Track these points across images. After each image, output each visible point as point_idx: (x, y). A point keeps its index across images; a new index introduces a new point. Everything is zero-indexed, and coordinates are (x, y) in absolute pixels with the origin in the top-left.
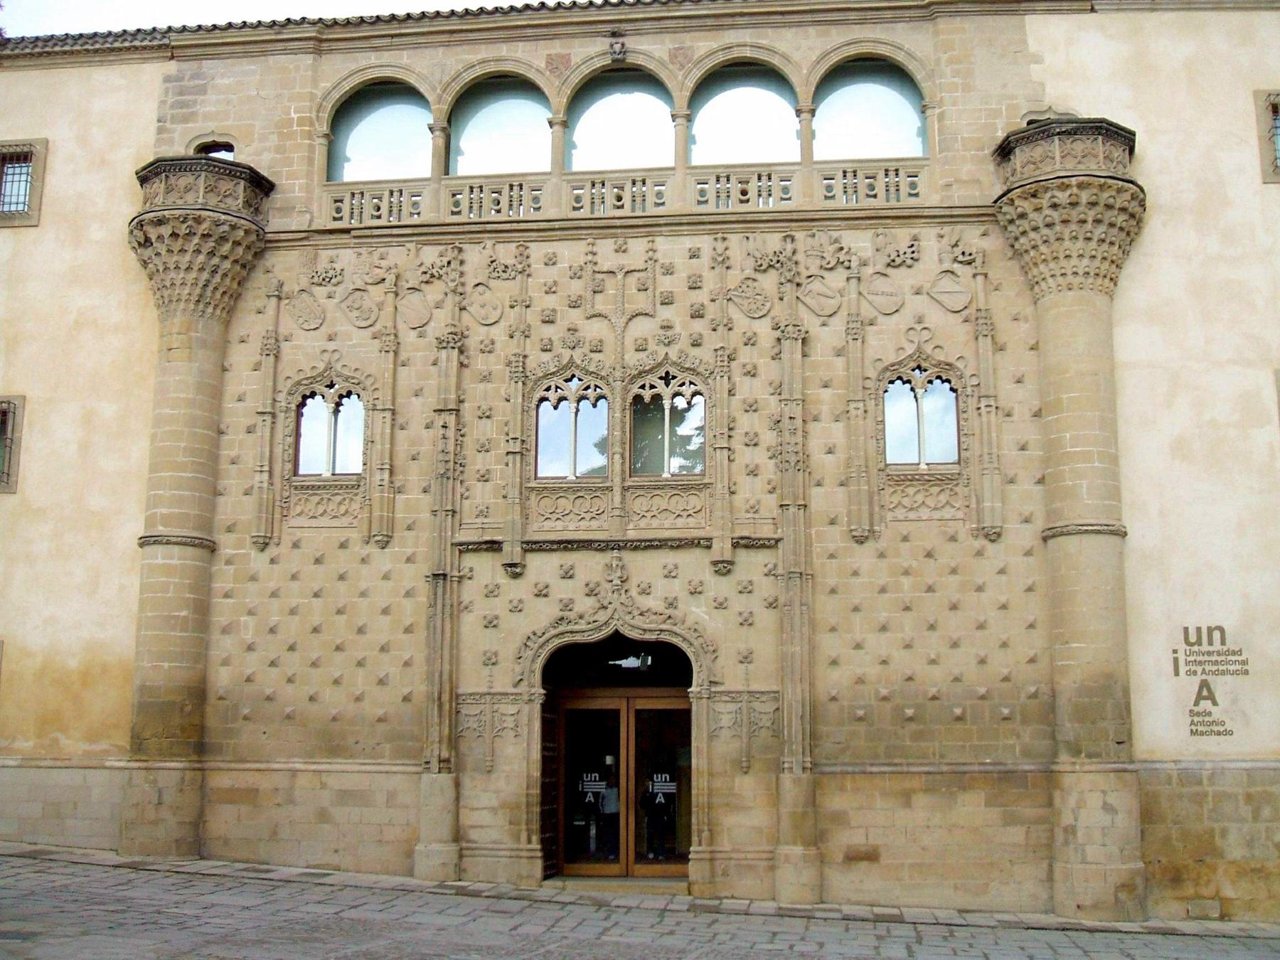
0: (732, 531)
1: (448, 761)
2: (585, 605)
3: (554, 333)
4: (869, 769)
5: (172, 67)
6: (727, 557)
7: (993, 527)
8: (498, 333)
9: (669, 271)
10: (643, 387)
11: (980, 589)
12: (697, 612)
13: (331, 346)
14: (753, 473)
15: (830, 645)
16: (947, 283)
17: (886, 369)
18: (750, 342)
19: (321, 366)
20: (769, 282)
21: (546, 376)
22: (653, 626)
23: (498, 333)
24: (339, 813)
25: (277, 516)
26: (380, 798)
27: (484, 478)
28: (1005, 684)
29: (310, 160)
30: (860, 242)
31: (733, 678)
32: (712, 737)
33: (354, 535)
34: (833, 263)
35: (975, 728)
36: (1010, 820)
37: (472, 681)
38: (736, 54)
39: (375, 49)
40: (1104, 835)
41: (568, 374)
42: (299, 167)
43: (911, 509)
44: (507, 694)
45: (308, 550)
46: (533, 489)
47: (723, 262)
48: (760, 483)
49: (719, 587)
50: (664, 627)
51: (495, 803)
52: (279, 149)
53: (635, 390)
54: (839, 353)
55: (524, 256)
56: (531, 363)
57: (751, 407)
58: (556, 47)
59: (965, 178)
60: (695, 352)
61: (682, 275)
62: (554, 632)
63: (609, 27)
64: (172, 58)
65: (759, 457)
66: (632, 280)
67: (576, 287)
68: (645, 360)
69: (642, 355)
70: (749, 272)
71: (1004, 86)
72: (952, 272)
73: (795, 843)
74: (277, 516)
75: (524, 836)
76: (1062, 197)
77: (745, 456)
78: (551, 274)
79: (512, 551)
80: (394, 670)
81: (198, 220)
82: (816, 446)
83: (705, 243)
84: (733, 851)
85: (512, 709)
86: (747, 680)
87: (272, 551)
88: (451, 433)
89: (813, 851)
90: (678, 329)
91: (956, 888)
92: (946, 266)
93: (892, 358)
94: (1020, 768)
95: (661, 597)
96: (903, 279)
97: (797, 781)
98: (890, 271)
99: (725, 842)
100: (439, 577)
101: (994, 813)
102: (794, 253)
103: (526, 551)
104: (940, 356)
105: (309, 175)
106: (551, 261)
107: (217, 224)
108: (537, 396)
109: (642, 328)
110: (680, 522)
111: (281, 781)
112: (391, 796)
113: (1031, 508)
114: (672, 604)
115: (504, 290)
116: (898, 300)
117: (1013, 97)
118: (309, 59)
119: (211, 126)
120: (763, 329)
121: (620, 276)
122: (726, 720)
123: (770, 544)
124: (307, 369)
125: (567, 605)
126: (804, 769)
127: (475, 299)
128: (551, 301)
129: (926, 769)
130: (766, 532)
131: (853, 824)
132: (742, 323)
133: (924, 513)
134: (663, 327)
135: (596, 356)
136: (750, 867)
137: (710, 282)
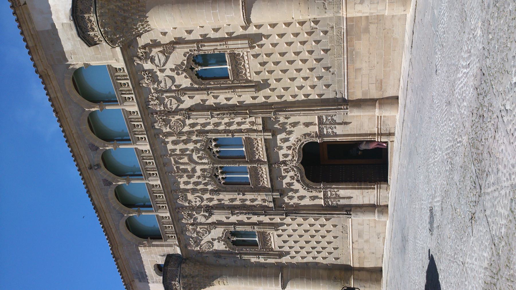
0: (260, 131)
2: (292, 173)
4: (346, 83)
7: (249, 44)
16: (157, 61)
19: (223, 243)
24: (366, 237)
25: (271, 253)
26: (360, 227)
29: (157, 246)
31: (315, 129)
32: (336, 135)
33: (275, 233)
36: (367, 30)
40: (373, 3)
42: (160, 249)
43: (246, 70)
45: (282, 244)
51: (361, 197)
52: (156, 254)
54: (191, 97)
59: (111, 54)
64: (133, 281)
71: (69, 39)
73: (375, 112)
79: (276, 195)
80: (317, 223)
81: (184, 284)
85: (329, 193)
89: (377, 105)
90: (192, 148)
91: (394, 50)
94: (345, 27)
95: (288, 148)
97: (351, 112)
99: (374, 130)
101: (364, 37)
104: (185, 62)
105: (162, 246)
108: (223, 185)
110: (260, 145)
111: (356, 252)
112: (359, 224)
115: (190, 196)
116: (167, 78)
117: (72, 35)
120: (188, 122)
122: (330, 130)
124: (225, 246)
125: (292, 178)
126: (347, 109)
130: (260, 121)
132: (186, 129)
133: (247, 66)
136: (383, 122)
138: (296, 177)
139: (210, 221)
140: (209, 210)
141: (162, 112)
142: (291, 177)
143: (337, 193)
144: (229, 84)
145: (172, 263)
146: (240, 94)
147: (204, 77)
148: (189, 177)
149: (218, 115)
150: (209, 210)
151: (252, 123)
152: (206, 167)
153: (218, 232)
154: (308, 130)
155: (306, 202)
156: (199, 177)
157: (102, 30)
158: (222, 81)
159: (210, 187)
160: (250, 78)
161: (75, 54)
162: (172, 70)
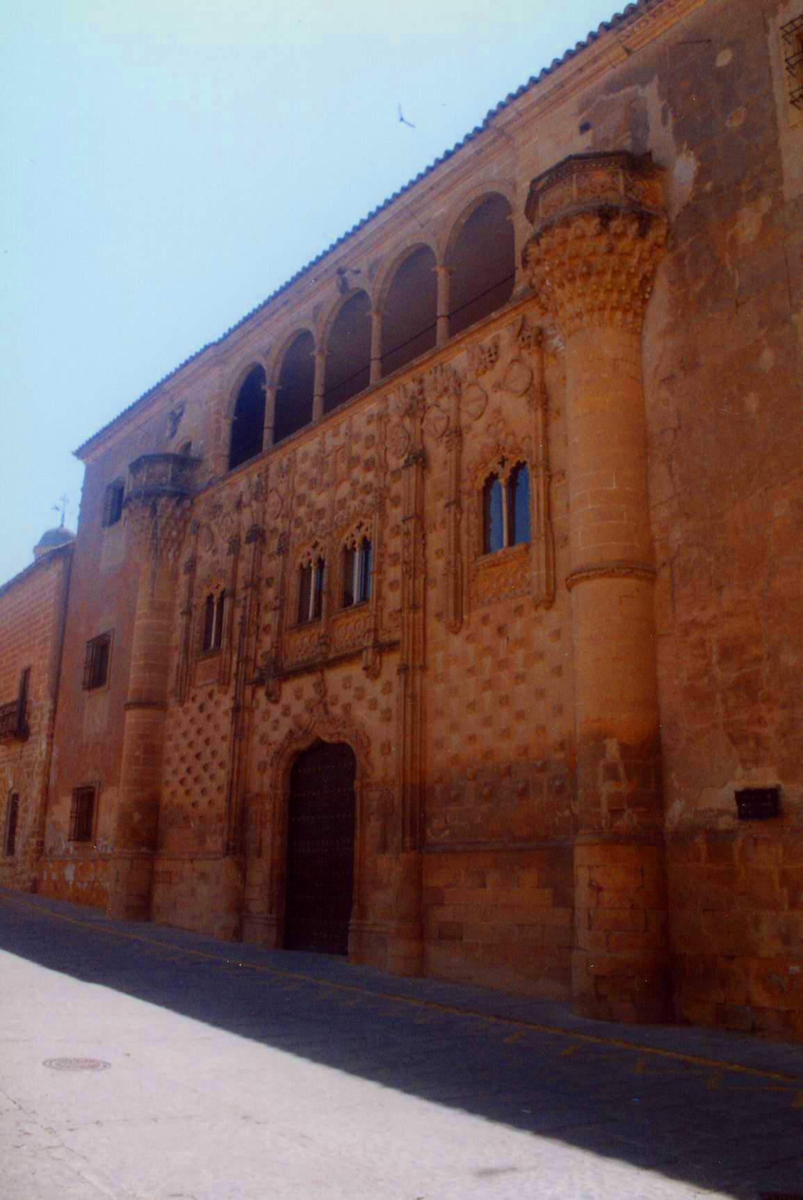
12: (360, 712)
15: (437, 728)
37: (255, 788)
48: (398, 593)
49: (375, 689)
53: (344, 540)
82: (431, 553)
84: (374, 924)
96: (488, 380)
102: (421, 392)
109: (345, 489)
114: (347, 708)
122: (375, 804)
123: (392, 646)
153: (225, 561)
154: (375, 753)
155: (260, 754)
158: (476, 534)
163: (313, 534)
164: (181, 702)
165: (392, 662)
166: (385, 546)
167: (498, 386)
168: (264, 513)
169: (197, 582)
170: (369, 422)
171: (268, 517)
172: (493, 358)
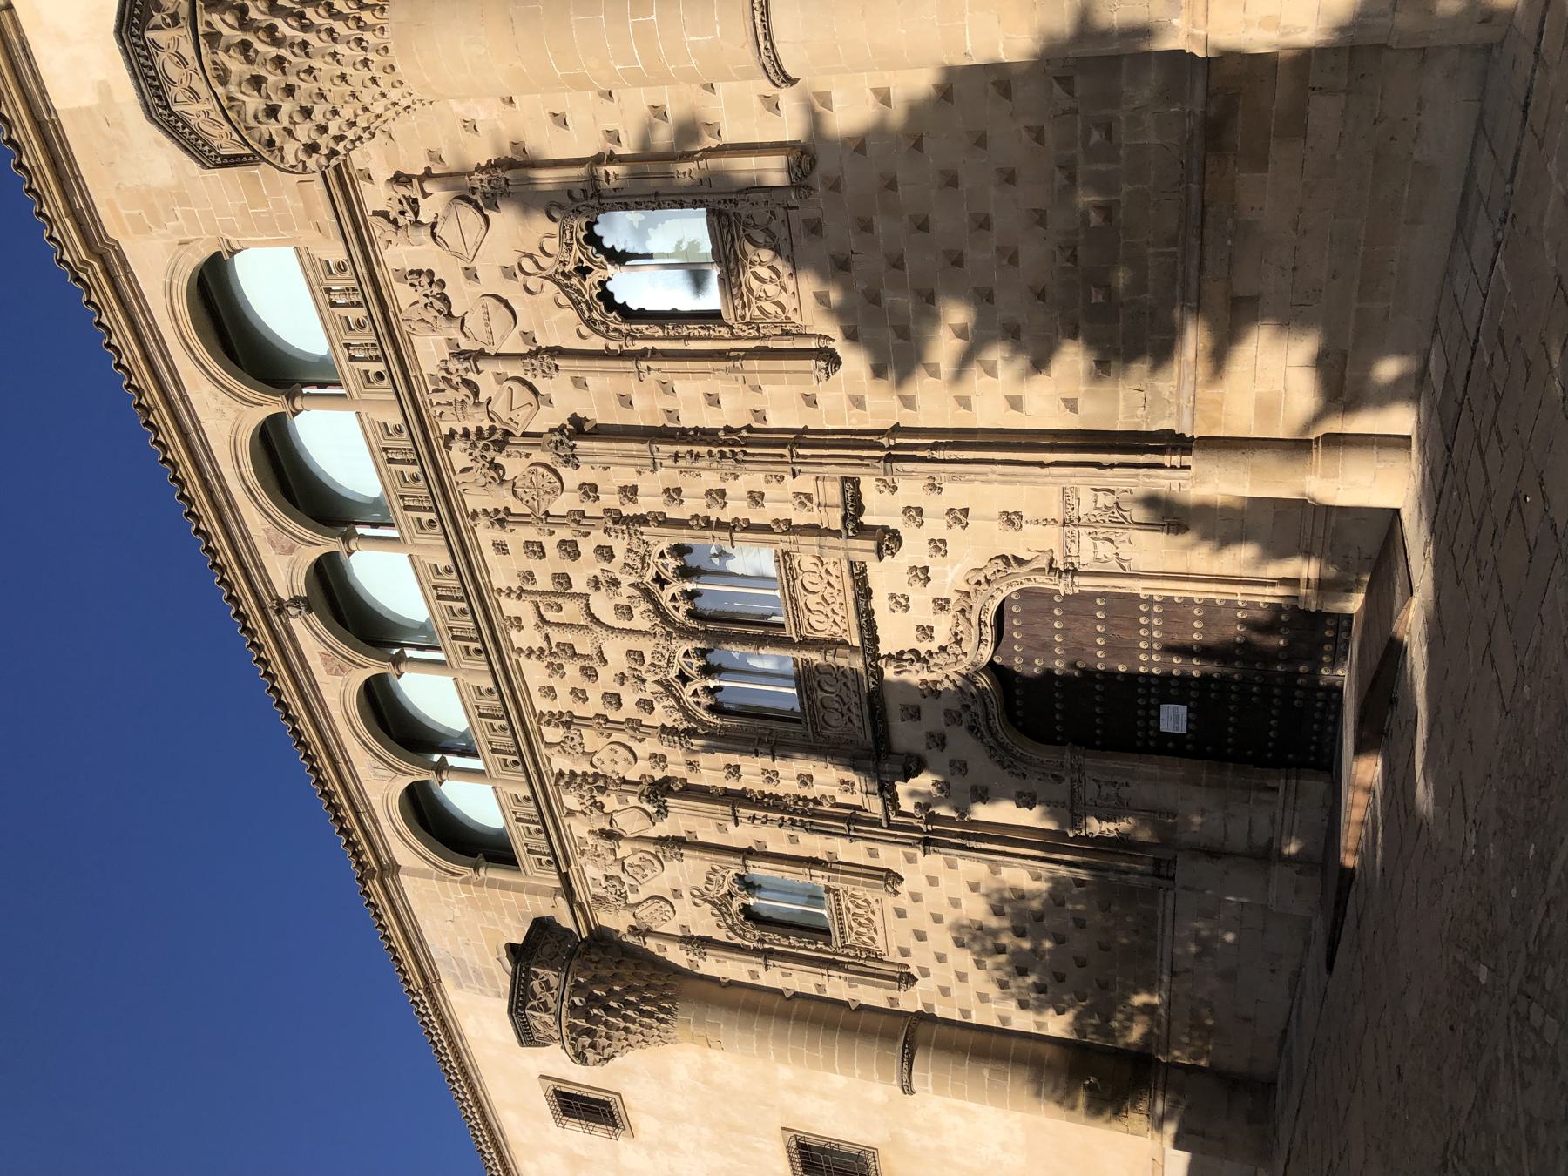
1: (1157, 863)
3: (629, 697)
5: (447, 984)
6: (872, 545)
8: (643, 750)
9: (528, 576)
10: (677, 609)
11: (892, 185)
12: (950, 577)
13: (686, 894)
14: (756, 498)
17: (590, 323)
18: (590, 491)
20: (514, 466)
21: (683, 708)
22: (975, 632)
23: (643, 750)
27: (806, 780)
28: (1049, 136)
30: (429, 351)
33: (890, 902)
34: (464, 390)
35: (1126, 188)
36: (1296, 125)
38: (253, 480)
39: (375, 822)
41: (677, 684)
44: (1073, 792)
45: (911, 943)
46: (816, 733)
47: (501, 519)
48: (771, 491)
49: (914, 549)
50: (975, 621)
52: (500, 911)
54: (580, 383)
55: (554, 719)
56: (669, 724)
57: (674, 494)
58: (315, 663)
60: (620, 553)
61: (533, 564)
62: (988, 739)
63: (275, 619)
65: (738, 489)
66: (550, 616)
67: (572, 668)
68: (640, 607)
69: (636, 612)
70: (506, 492)
72: (434, 225)
74: (876, 965)
75: (1264, 796)
76: (253, 103)
77: (737, 508)
78: (562, 690)
83: (486, 535)
86: (1046, 522)
87: (914, 971)
88: (760, 814)
92: (425, 233)
93: (573, 313)
98: (456, 312)
100: (927, 843)
103: (890, 751)
106: (549, 692)
107: (573, 1007)
109: (602, 605)
113: (756, 99)
114: (941, 605)
118: (404, 879)
119: (492, 959)
121: (549, 630)
122: (1105, 549)
127: (606, 768)
128: (594, 695)
129: (1193, 273)
130: (833, 492)
131: (1279, 387)
134: (597, 588)
135: (648, 659)
137: (531, 533)
138: (965, 717)
139: (663, 828)
140: (660, 791)
141: (486, 434)
142: (947, 713)
143: (1125, 793)
144: (721, 338)
145: (547, 950)
146: (758, 379)
147: (634, 306)
148: (589, 673)
149: (676, 457)
150: (660, 791)
151: (805, 499)
152: (647, 646)
156: (622, 678)
157: (220, 90)
159: (663, 715)
160: (795, 318)
161: (184, 200)
162: (508, 273)
163: (666, 686)
164: (910, 979)
165: (879, 509)
166: (696, 517)
167: (471, 274)
168: (624, 781)
169: (720, 935)
170: (501, 547)
171: (632, 775)
172: (425, 280)
